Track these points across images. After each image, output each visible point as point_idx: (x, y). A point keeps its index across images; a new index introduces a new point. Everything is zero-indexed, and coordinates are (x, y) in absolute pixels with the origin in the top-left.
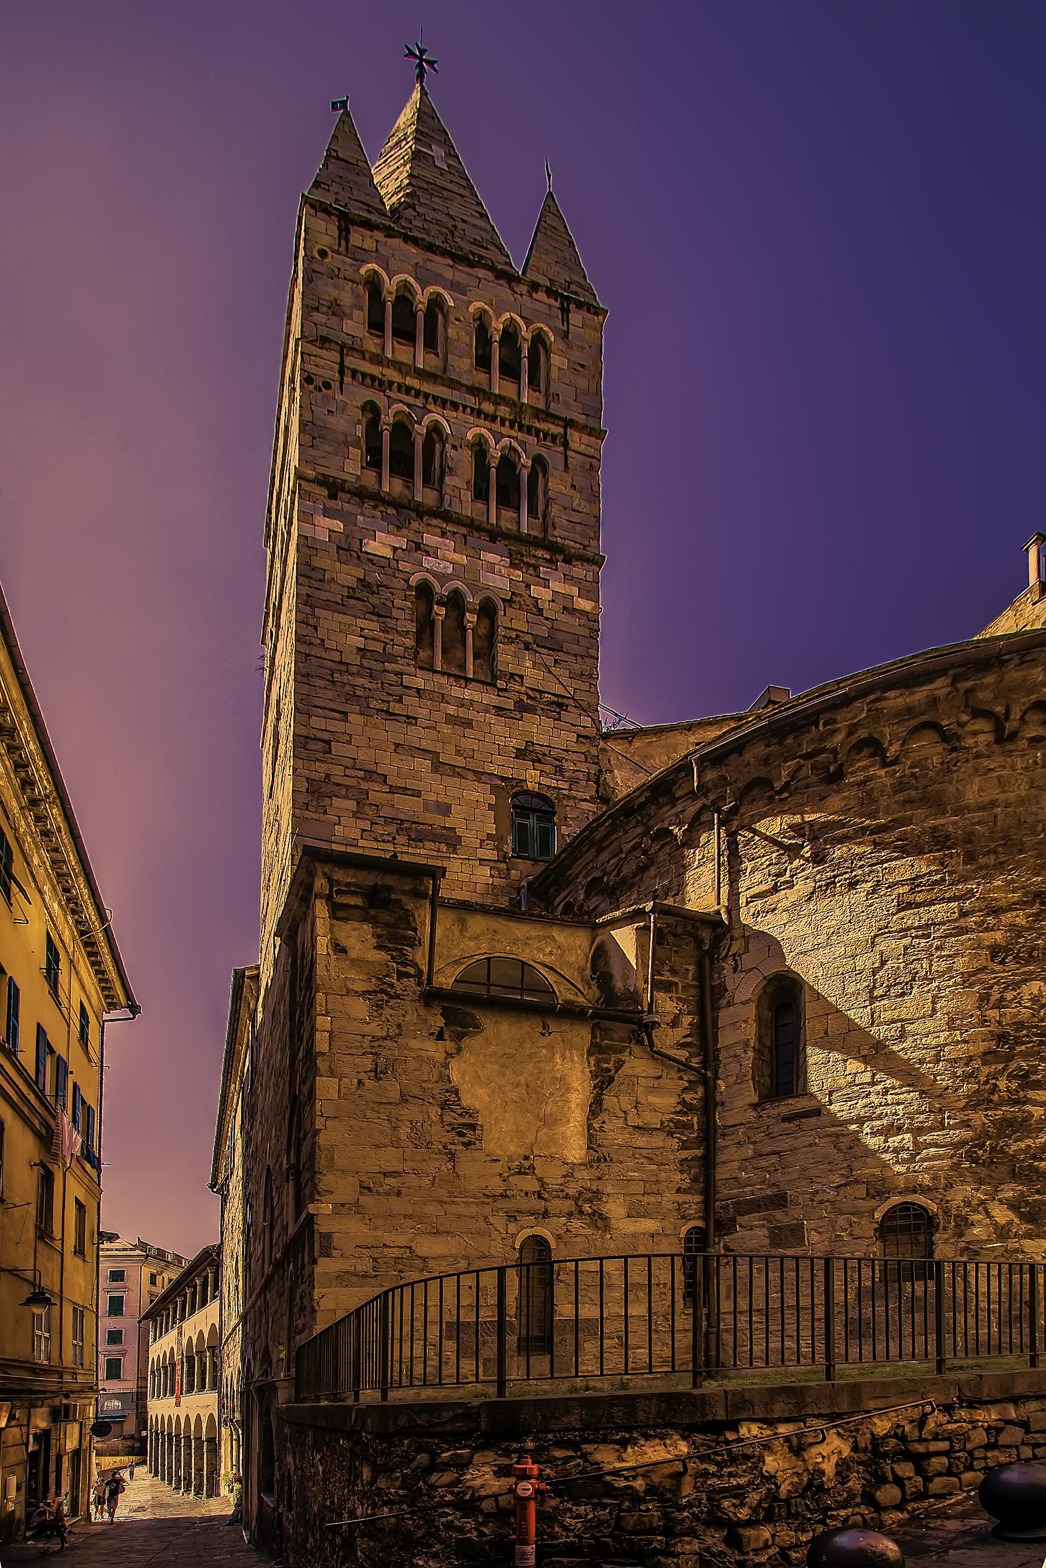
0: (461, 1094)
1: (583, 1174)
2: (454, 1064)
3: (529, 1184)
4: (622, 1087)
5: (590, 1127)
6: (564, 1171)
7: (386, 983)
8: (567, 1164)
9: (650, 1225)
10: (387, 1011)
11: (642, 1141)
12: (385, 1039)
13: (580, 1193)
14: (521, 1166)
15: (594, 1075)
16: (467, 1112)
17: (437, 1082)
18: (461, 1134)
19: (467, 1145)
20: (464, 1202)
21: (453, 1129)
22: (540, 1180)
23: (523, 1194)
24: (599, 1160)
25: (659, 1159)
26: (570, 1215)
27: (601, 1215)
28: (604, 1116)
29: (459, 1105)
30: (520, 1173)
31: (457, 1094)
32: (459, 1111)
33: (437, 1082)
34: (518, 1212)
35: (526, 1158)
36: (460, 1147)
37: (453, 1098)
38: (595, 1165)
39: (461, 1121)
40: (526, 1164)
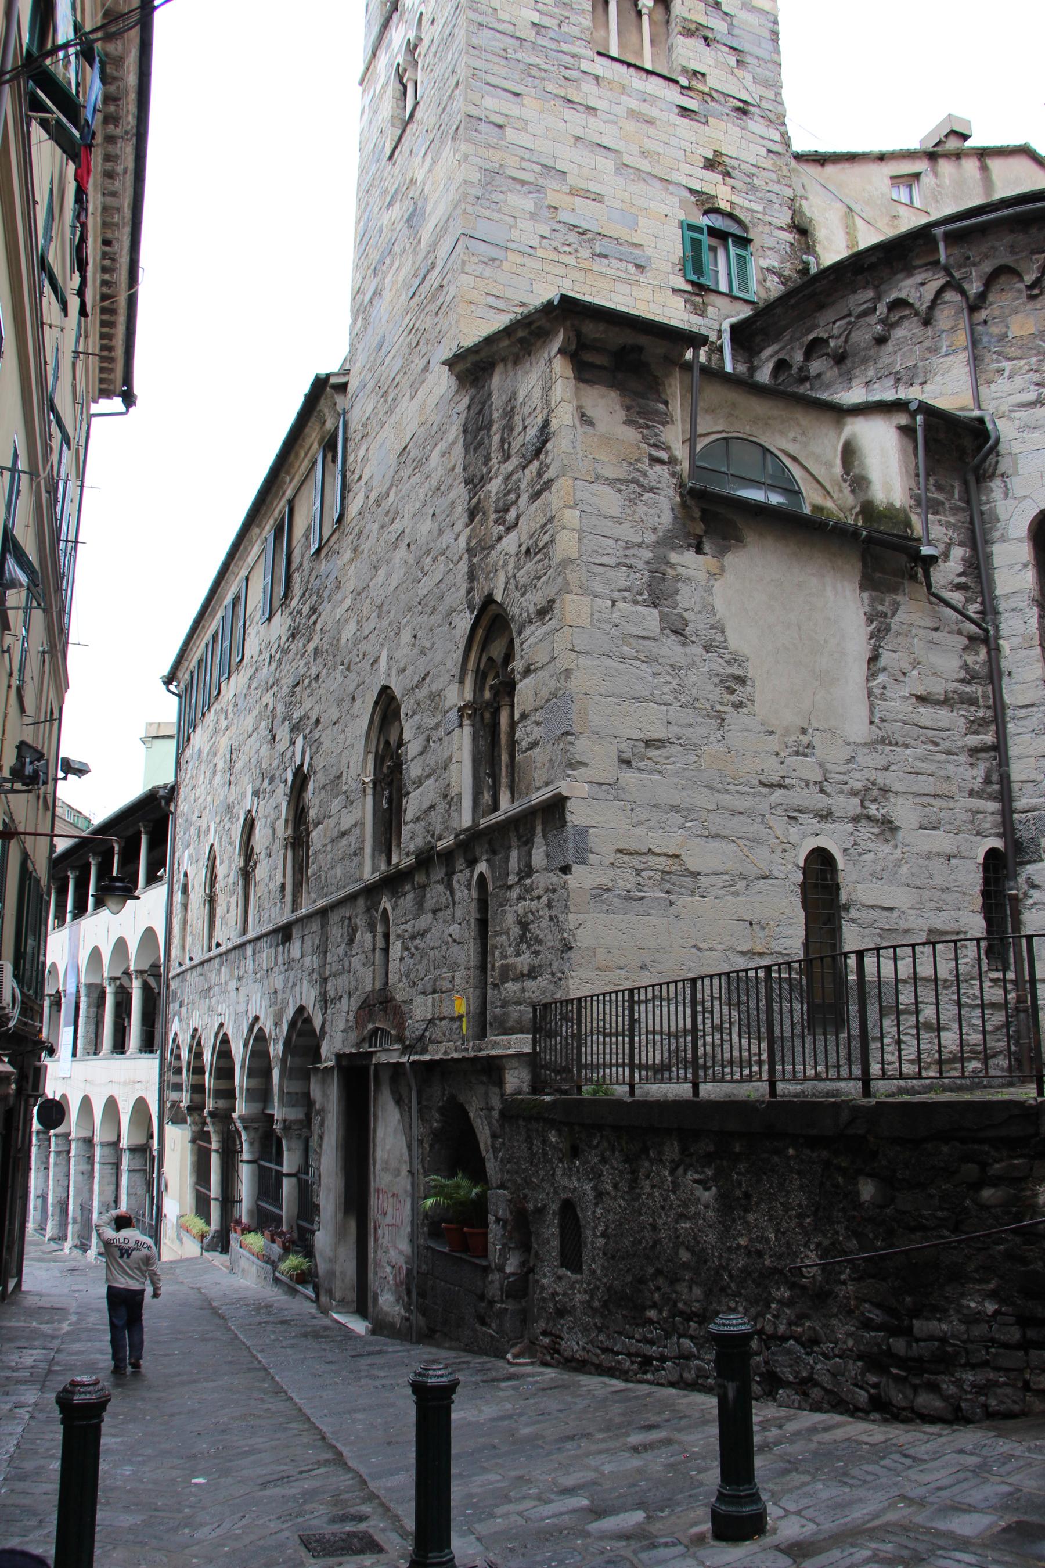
0: (728, 633)
1: (868, 759)
2: (718, 586)
3: (807, 768)
4: (900, 639)
5: (870, 693)
6: (846, 753)
7: (637, 470)
8: (848, 744)
9: (941, 841)
10: (641, 509)
11: (926, 714)
12: (639, 546)
13: (867, 790)
14: (798, 743)
15: (870, 620)
16: (736, 660)
17: (700, 612)
18: (732, 691)
19: (738, 705)
20: (738, 792)
21: (721, 681)
22: (821, 765)
23: (803, 785)
24: (882, 741)
25: (944, 745)
26: (856, 819)
27: (891, 822)
28: (881, 678)
29: (725, 648)
30: (797, 753)
31: (723, 632)
32: (727, 657)
33: (700, 612)
34: (800, 811)
35: (804, 731)
36: (729, 709)
37: (719, 637)
38: (879, 747)
39: (730, 671)
40: (805, 740)
